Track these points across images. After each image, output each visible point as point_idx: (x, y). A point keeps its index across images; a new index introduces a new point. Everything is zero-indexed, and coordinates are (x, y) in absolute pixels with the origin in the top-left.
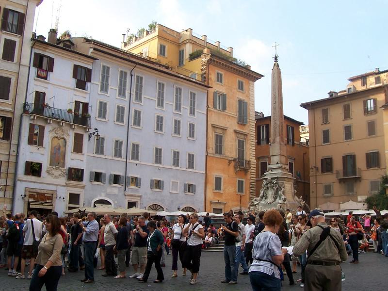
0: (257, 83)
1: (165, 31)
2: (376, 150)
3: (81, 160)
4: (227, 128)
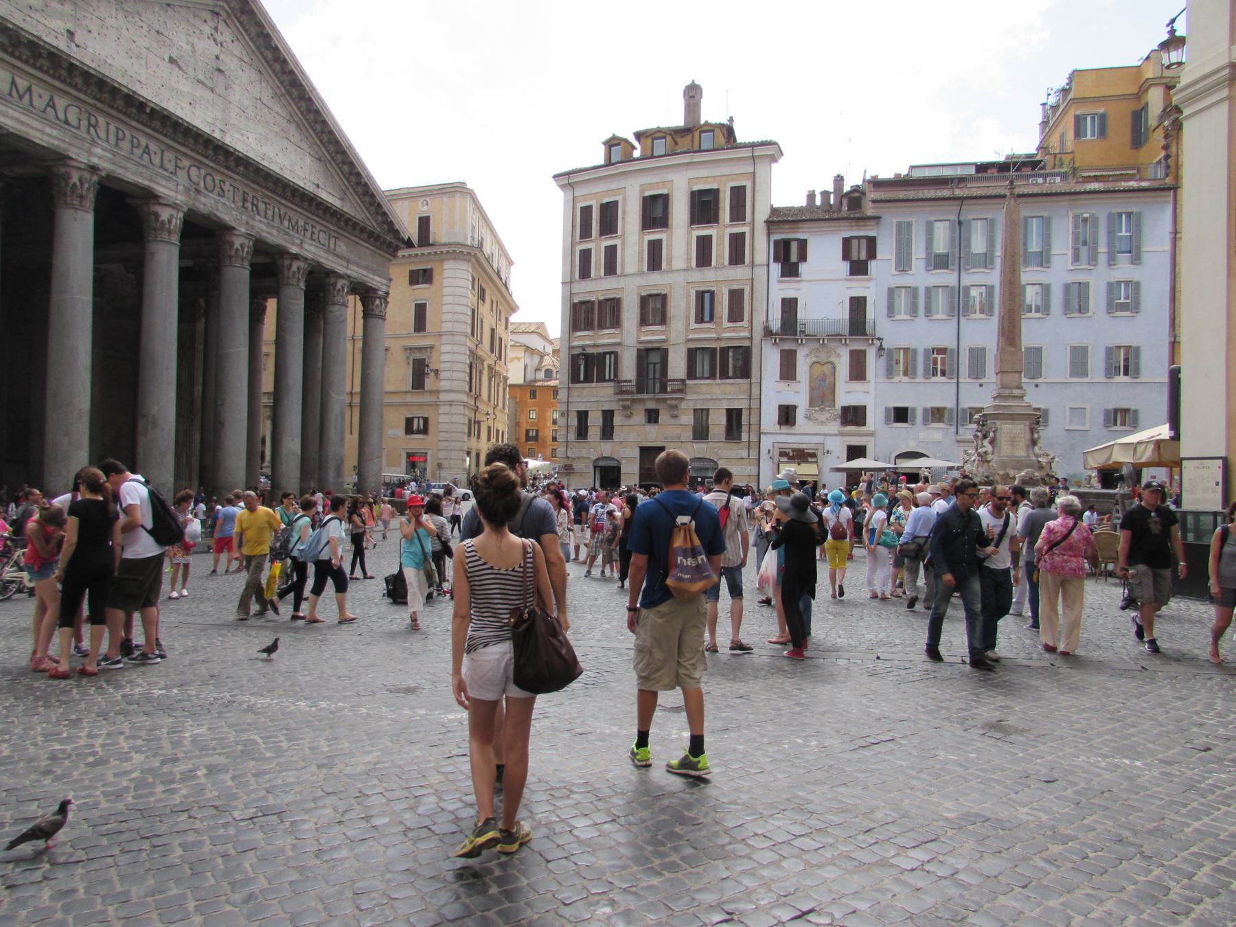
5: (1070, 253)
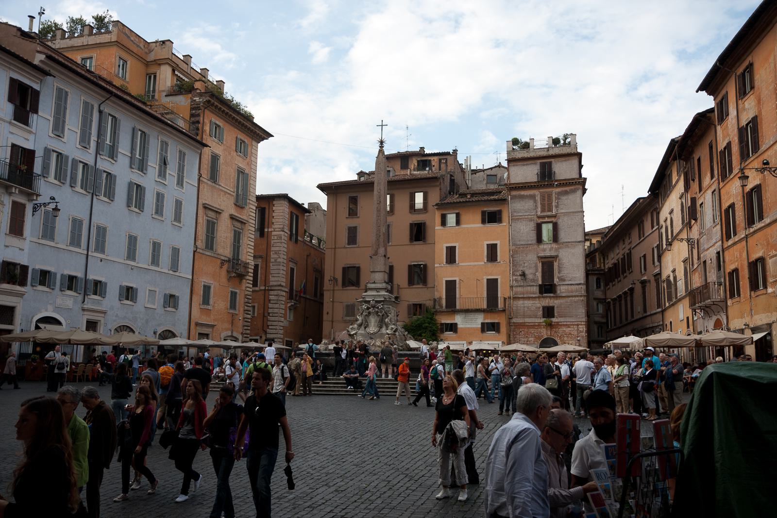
0: (262, 145)
1: (126, 35)
2: (422, 261)
3: (20, 249)
4: (223, 211)
5: (157, 168)
